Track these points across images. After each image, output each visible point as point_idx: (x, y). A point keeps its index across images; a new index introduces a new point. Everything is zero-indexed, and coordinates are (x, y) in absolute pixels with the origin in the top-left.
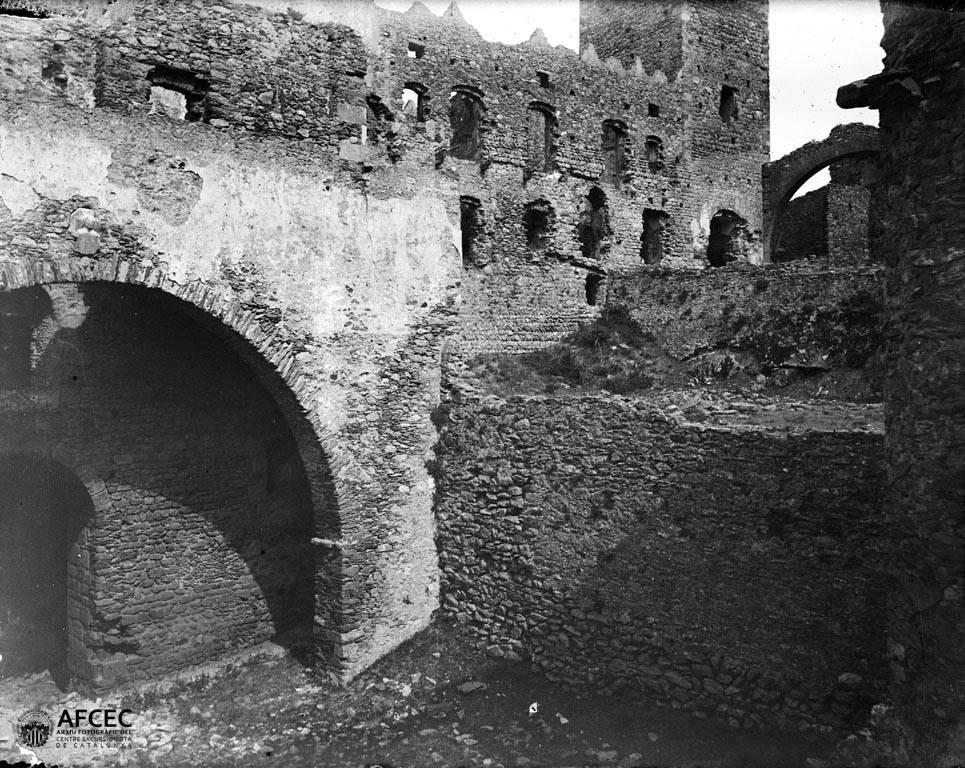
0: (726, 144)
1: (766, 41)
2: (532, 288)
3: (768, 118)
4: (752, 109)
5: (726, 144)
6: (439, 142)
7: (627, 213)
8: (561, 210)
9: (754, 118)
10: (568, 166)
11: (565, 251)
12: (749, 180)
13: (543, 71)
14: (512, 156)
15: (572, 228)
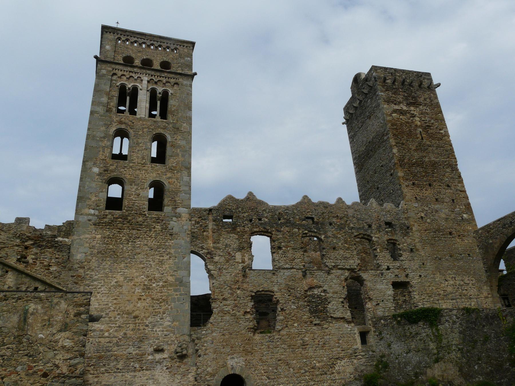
0: (446, 236)
1: (460, 177)
2: (317, 341)
3: (473, 217)
4: (459, 214)
5: (446, 236)
6: (244, 263)
7: (379, 286)
8: (331, 291)
9: (462, 219)
10: (333, 264)
11: (338, 315)
12: (469, 255)
13: (310, 216)
14: (293, 264)
15: (341, 300)
